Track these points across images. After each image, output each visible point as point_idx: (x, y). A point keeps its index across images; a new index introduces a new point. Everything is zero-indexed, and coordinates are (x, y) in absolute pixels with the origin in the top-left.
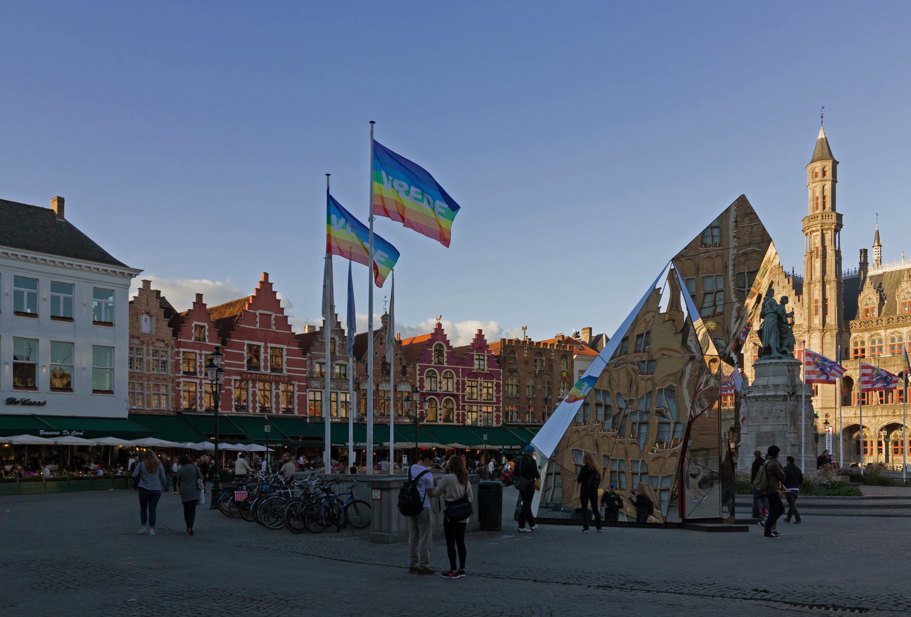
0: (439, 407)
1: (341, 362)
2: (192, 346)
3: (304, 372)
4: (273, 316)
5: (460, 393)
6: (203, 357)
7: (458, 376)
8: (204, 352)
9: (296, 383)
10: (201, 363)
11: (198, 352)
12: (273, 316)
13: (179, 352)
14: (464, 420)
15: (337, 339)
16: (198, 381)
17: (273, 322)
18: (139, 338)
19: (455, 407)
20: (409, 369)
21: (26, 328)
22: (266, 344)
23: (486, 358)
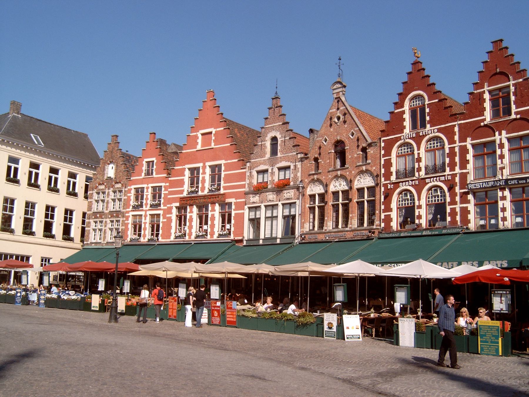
0: (417, 203)
1: (283, 164)
2: (142, 181)
3: (243, 186)
4: (214, 132)
5: (457, 170)
6: (150, 190)
7: (451, 141)
8: (150, 185)
9: (233, 200)
10: (147, 195)
11: (145, 186)
12: (214, 132)
13: (131, 189)
14: (465, 221)
15: (279, 136)
16: (143, 213)
17: (213, 138)
18: (103, 184)
19: (448, 199)
20: (370, 151)
21: (11, 191)
22: (204, 164)
23: (512, 89)
